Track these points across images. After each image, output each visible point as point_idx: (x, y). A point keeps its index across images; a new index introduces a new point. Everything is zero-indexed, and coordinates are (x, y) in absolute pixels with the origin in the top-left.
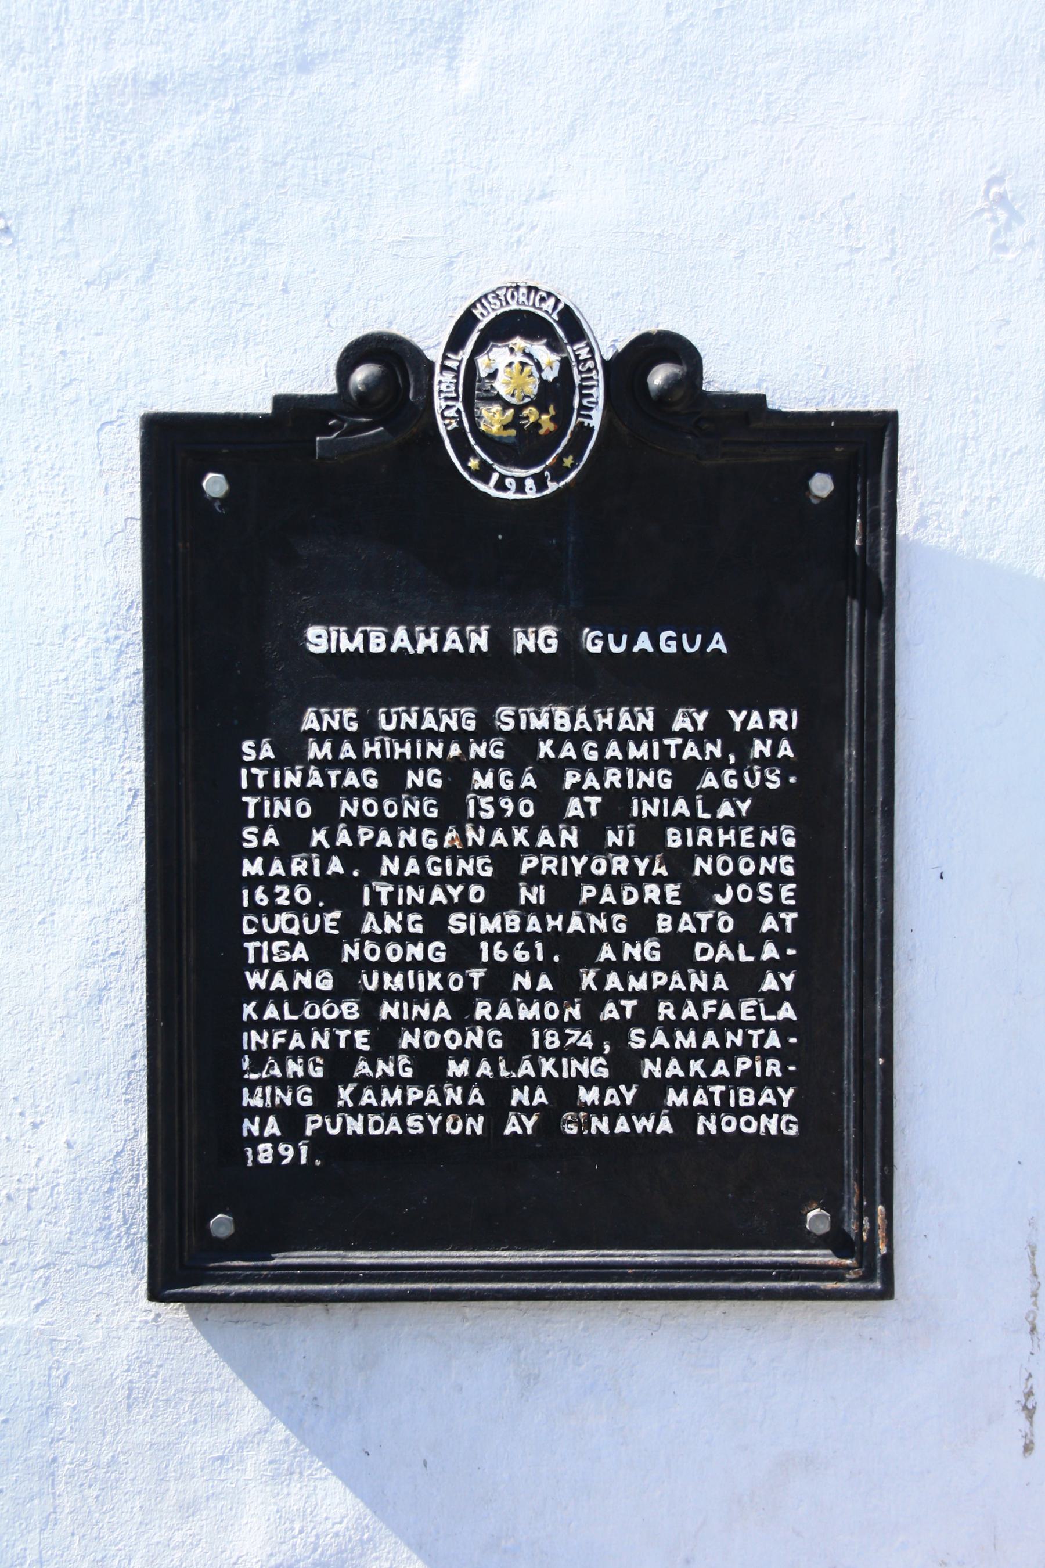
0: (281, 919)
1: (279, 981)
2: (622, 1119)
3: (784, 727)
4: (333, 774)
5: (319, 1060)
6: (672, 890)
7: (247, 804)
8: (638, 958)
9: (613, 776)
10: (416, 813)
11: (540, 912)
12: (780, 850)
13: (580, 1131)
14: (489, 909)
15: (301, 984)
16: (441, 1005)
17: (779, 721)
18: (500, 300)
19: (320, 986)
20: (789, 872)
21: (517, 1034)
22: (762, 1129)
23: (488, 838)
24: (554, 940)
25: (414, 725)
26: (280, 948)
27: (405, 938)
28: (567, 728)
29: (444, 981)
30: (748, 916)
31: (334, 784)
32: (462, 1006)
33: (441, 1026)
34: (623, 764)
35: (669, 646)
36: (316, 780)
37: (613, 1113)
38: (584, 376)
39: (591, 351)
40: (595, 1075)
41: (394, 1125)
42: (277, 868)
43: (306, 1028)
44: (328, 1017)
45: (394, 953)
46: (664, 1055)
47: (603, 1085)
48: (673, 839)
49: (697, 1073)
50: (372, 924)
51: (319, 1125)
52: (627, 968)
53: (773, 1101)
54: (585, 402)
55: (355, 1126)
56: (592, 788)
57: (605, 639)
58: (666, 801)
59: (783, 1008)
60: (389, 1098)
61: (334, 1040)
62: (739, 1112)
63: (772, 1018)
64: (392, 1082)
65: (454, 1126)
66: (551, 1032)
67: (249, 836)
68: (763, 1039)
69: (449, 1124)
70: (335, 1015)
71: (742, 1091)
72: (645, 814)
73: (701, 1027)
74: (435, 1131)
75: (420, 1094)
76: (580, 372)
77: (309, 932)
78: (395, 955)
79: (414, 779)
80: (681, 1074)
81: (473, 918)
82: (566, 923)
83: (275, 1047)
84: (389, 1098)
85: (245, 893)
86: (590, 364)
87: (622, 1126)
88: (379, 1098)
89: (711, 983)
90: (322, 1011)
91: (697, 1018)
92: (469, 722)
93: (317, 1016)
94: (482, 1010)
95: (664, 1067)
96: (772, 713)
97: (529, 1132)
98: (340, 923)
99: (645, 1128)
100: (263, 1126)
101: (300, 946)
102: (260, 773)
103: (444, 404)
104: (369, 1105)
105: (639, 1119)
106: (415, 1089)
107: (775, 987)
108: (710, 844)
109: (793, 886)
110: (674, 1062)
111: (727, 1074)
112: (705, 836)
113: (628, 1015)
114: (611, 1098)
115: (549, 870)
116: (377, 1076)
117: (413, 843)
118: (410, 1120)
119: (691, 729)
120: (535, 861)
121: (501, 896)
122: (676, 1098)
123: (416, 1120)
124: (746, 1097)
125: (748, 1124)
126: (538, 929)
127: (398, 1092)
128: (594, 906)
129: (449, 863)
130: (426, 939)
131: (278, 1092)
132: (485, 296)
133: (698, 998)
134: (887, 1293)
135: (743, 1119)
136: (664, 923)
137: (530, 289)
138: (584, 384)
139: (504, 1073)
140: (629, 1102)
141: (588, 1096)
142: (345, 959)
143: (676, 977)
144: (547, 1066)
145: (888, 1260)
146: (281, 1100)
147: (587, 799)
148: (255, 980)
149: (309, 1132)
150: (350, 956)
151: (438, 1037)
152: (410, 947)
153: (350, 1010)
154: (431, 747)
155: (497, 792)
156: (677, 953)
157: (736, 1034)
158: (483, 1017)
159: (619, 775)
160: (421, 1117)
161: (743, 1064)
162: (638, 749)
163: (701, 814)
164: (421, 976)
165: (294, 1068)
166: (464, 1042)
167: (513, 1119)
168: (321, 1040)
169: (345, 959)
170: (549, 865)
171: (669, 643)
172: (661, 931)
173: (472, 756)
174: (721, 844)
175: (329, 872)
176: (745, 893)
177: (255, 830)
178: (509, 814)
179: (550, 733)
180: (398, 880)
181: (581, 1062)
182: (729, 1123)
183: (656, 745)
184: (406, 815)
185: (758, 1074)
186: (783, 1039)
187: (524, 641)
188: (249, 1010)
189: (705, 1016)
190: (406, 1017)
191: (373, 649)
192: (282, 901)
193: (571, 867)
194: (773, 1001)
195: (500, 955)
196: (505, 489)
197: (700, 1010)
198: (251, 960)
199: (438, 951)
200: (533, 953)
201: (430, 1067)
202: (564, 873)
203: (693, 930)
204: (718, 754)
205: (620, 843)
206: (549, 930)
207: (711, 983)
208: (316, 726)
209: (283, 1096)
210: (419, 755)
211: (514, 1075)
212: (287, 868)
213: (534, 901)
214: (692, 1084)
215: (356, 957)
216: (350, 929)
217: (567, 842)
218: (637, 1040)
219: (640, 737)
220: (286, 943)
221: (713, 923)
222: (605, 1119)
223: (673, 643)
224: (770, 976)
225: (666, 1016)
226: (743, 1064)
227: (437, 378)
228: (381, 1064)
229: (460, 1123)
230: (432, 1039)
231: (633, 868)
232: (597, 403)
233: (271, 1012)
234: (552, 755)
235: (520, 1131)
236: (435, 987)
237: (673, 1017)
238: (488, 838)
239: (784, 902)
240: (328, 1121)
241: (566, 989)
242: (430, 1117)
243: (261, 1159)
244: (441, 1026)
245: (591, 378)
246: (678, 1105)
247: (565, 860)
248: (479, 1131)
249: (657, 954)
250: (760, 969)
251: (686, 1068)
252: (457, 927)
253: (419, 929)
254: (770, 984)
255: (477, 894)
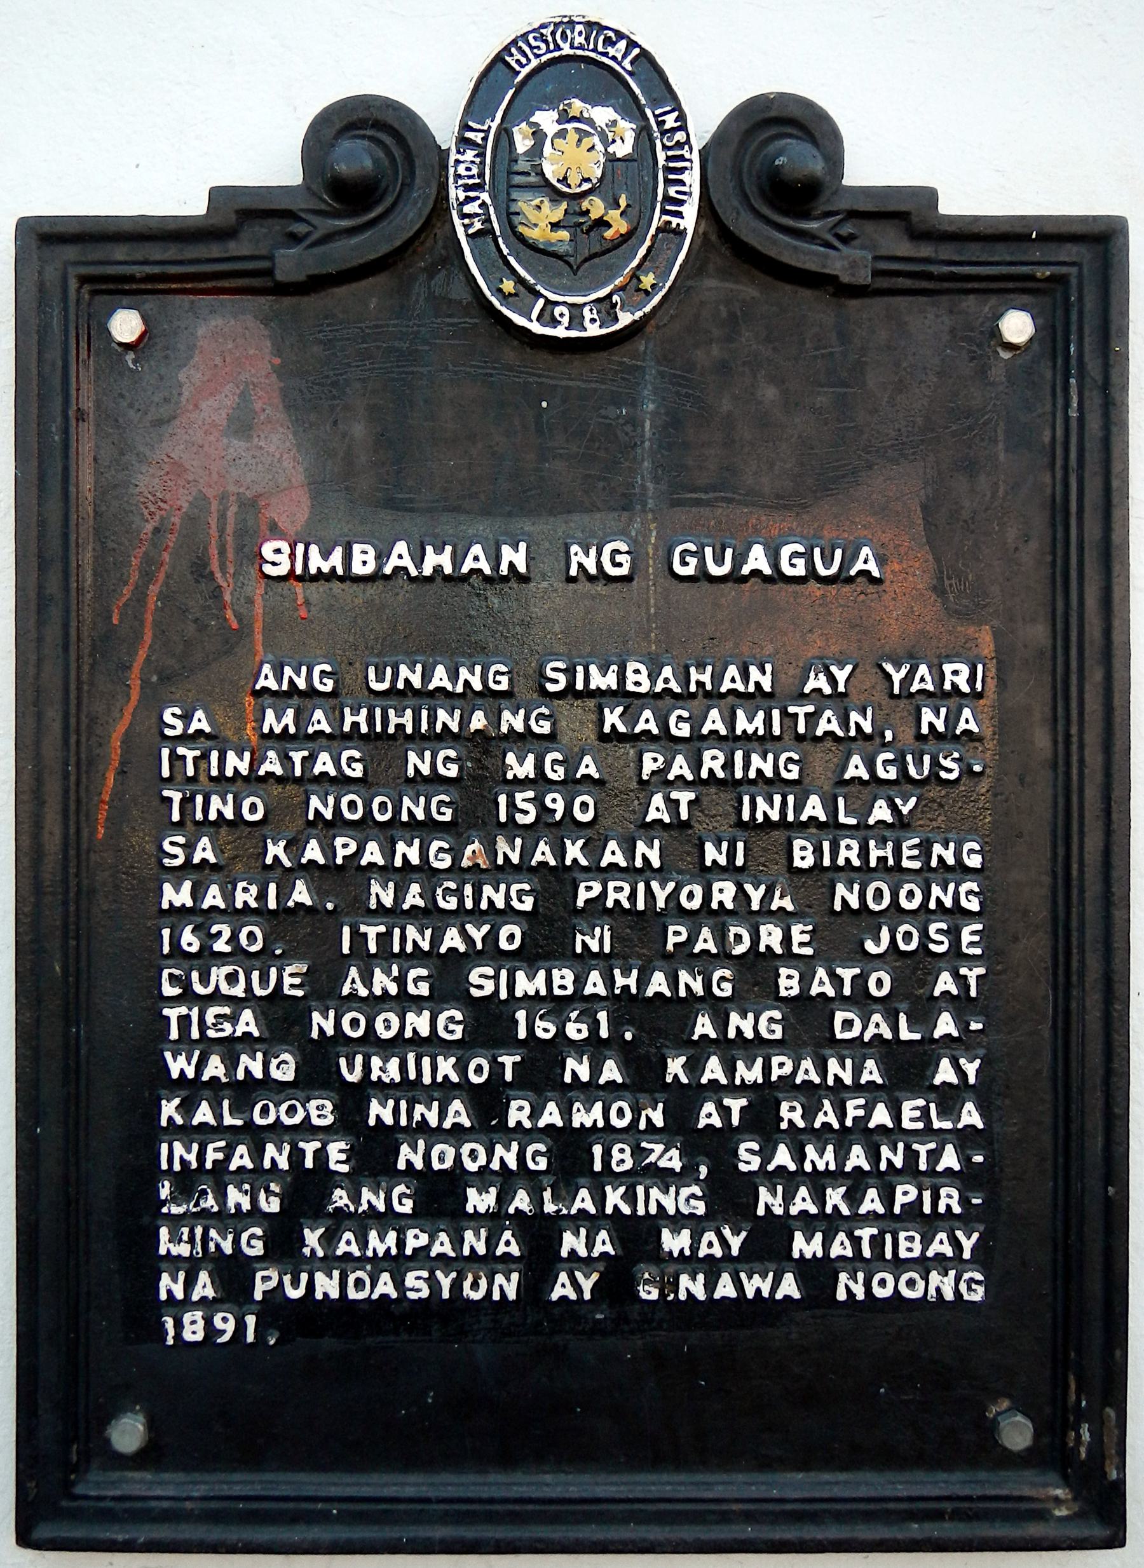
0: (218, 974)
1: (215, 1068)
2: (725, 1278)
3: (965, 688)
4: (297, 757)
5: (274, 1187)
6: (799, 933)
7: (170, 800)
8: (749, 1034)
9: (713, 761)
10: (420, 815)
11: (605, 962)
12: (962, 870)
13: (662, 1295)
14: (530, 956)
15: (247, 1071)
16: (457, 1105)
17: (956, 679)
18: (546, 42)
19: (276, 1074)
20: (974, 905)
21: (571, 1153)
22: (932, 1292)
23: (527, 852)
24: (625, 1005)
25: (417, 682)
26: (216, 1017)
27: (404, 1002)
28: (644, 689)
29: (461, 1067)
30: (913, 969)
31: (298, 772)
32: (488, 1103)
33: (457, 1134)
34: (730, 741)
35: (793, 565)
36: (272, 765)
37: (712, 1268)
38: (670, 153)
39: (682, 118)
40: (685, 1211)
41: (385, 1286)
42: (213, 897)
43: (256, 1137)
44: (288, 1121)
45: (386, 1026)
46: (788, 1180)
47: (696, 1224)
48: (803, 858)
49: (835, 1207)
50: (353, 981)
51: (273, 1283)
52: (733, 1049)
53: (948, 1251)
54: (672, 191)
55: (327, 1286)
56: (680, 777)
57: (700, 554)
58: (791, 799)
59: (965, 1111)
60: (380, 1244)
61: (297, 1156)
62: (898, 1265)
63: (948, 1125)
64: (387, 1219)
65: (475, 1286)
66: (620, 1146)
67: (173, 848)
68: (934, 1156)
69: (467, 1284)
70: (297, 1119)
71: (902, 1235)
72: (760, 818)
73: (842, 1138)
74: (446, 1295)
75: (424, 1239)
76: (665, 147)
77: (259, 992)
78: (388, 1028)
79: (417, 762)
80: (813, 1210)
81: (504, 974)
82: (643, 982)
83: (209, 1165)
84: (380, 1244)
85: (166, 933)
86: (680, 136)
87: (725, 1288)
88: (363, 1243)
89: (857, 1071)
90: (278, 1113)
91: (836, 1126)
92: (498, 678)
93: (271, 1119)
94: (518, 1113)
95: (788, 1199)
96: (948, 668)
97: (587, 1296)
98: (308, 977)
99: (758, 1291)
100: (189, 1285)
101: (247, 1015)
102: (190, 754)
103: (462, 196)
104: (348, 1256)
105: (750, 1278)
106: (417, 1231)
107: (953, 1079)
108: (856, 862)
109: (979, 927)
110: (803, 1191)
111: (881, 1210)
112: (849, 851)
113: (735, 1121)
114: (710, 1245)
115: (617, 902)
116: (360, 1210)
117: (415, 860)
118: (410, 1280)
119: (827, 690)
120: (597, 888)
121: (547, 940)
122: (805, 1246)
123: (418, 1278)
124: (909, 1245)
125: (911, 1283)
126: (601, 991)
127: (392, 1237)
128: (685, 955)
129: (468, 890)
130: (434, 1002)
131: (213, 1233)
132: (525, 36)
133: (839, 1092)
134: (1116, 1540)
135: (905, 1277)
136: (788, 983)
137: (590, 25)
138: (671, 165)
139: (550, 1208)
140: (735, 1252)
141: (675, 1242)
142: (315, 1035)
143: (807, 1064)
144: (614, 1197)
145: (1118, 1491)
146: (218, 1246)
147: (674, 795)
148: (178, 1065)
149: (258, 1296)
150: (321, 1029)
151: (451, 1152)
152: (410, 1017)
153: (321, 1111)
154: (442, 715)
155: (540, 781)
156: (809, 1024)
157: (894, 1150)
158: (519, 1123)
159: (721, 760)
160: (425, 1274)
161: (905, 1194)
162: (750, 720)
163: (842, 819)
164: (426, 1062)
165: (236, 1197)
166: (489, 1161)
167: (563, 1277)
168: (276, 1155)
169: (315, 1035)
170: (618, 894)
171: (794, 561)
172: (783, 993)
173: (504, 729)
174: (873, 863)
175: (291, 904)
176: (908, 936)
177: (181, 840)
178: (558, 816)
179: (620, 694)
180: (395, 914)
181: (666, 1192)
182: (883, 1283)
183: (776, 714)
184: (405, 817)
185: (927, 1209)
186: (965, 1159)
187: (582, 559)
188: (169, 1109)
189: (849, 1123)
190: (403, 1122)
191: (358, 569)
192: (221, 946)
193: (650, 894)
194: (949, 1099)
195: (545, 1030)
196: (555, 323)
197: (842, 1114)
198: (174, 1034)
199: (451, 1023)
200: (595, 1026)
201: (440, 1197)
202: (641, 906)
203: (831, 993)
204: (867, 728)
205: (722, 860)
206: (617, 992)
207: (857, 1071)
208: (272, 684)
209: (219, 1240)
210: (424, 727)
211: (565, 1212)
212: (229, 897)
213: (595, 948)
214: (827, 1224)
215: (330, 1031)
216: (324, 988)
217: (645, 858)
218: (748, 1159)
219: (757, 699)
220: (226, 1010)
221: (860, 981)
222: (701, 1277)
223: (800, 562)
224: (945, 1063)
225: (790, 1121)
226: (905, 1194)
227: (453, 156)
228: (366, 1195)
229: (483, 1283)
230: (443, 1156)
231: (742, 896)
232: (690, 194)
233: (204, 1114)
234: (622, 729)
235: (573, 1296)
236: (446, 1077)
237: (801, 1124)
238: (527, 852)
239: (965, 950)
240: (287, 1279)
241: (644, 1079)
242: (439, 1274)
243: (188, 1336)
244: (457, 1134)
245: (681, 158)
246: (808, 1256)
247: (641, 887)
248: (512, 1295)
249: (778, 1029)
250: (926, 1053)
251: (821, 1200)
252: (480, 987)
253: (424, 989)
254: (945, 1073)
255: (510, 936)
